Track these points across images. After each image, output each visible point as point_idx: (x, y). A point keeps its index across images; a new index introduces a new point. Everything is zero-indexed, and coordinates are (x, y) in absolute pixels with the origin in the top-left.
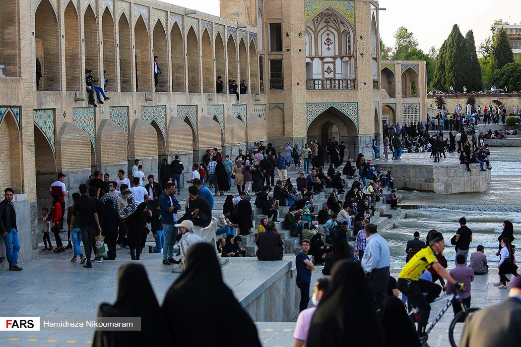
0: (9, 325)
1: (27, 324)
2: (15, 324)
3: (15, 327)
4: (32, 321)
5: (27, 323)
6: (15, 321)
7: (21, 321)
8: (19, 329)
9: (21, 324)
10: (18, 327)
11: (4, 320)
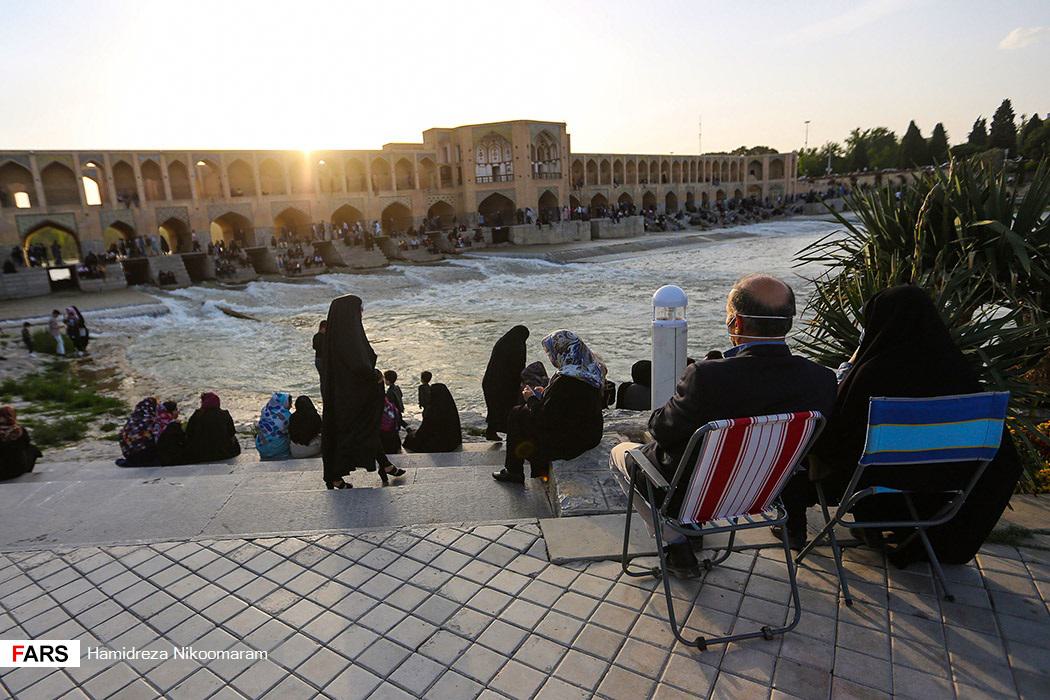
0: (17, 656)
1: (54, 655)
2: (31, 654)
3: (31, 661)
4: (65, 649)
5: (54, 651)
6: (31, 648)
7: (42, 647)
8: (39, 664)
9: (42, 654)
10: (36, 660)
11: (6, 645)
